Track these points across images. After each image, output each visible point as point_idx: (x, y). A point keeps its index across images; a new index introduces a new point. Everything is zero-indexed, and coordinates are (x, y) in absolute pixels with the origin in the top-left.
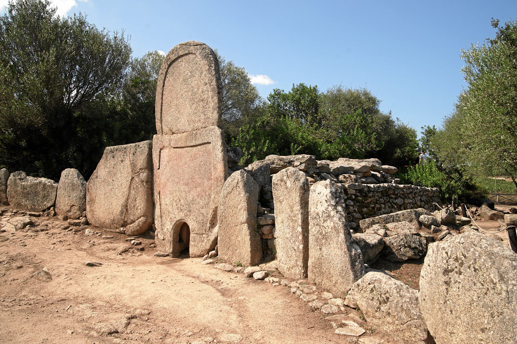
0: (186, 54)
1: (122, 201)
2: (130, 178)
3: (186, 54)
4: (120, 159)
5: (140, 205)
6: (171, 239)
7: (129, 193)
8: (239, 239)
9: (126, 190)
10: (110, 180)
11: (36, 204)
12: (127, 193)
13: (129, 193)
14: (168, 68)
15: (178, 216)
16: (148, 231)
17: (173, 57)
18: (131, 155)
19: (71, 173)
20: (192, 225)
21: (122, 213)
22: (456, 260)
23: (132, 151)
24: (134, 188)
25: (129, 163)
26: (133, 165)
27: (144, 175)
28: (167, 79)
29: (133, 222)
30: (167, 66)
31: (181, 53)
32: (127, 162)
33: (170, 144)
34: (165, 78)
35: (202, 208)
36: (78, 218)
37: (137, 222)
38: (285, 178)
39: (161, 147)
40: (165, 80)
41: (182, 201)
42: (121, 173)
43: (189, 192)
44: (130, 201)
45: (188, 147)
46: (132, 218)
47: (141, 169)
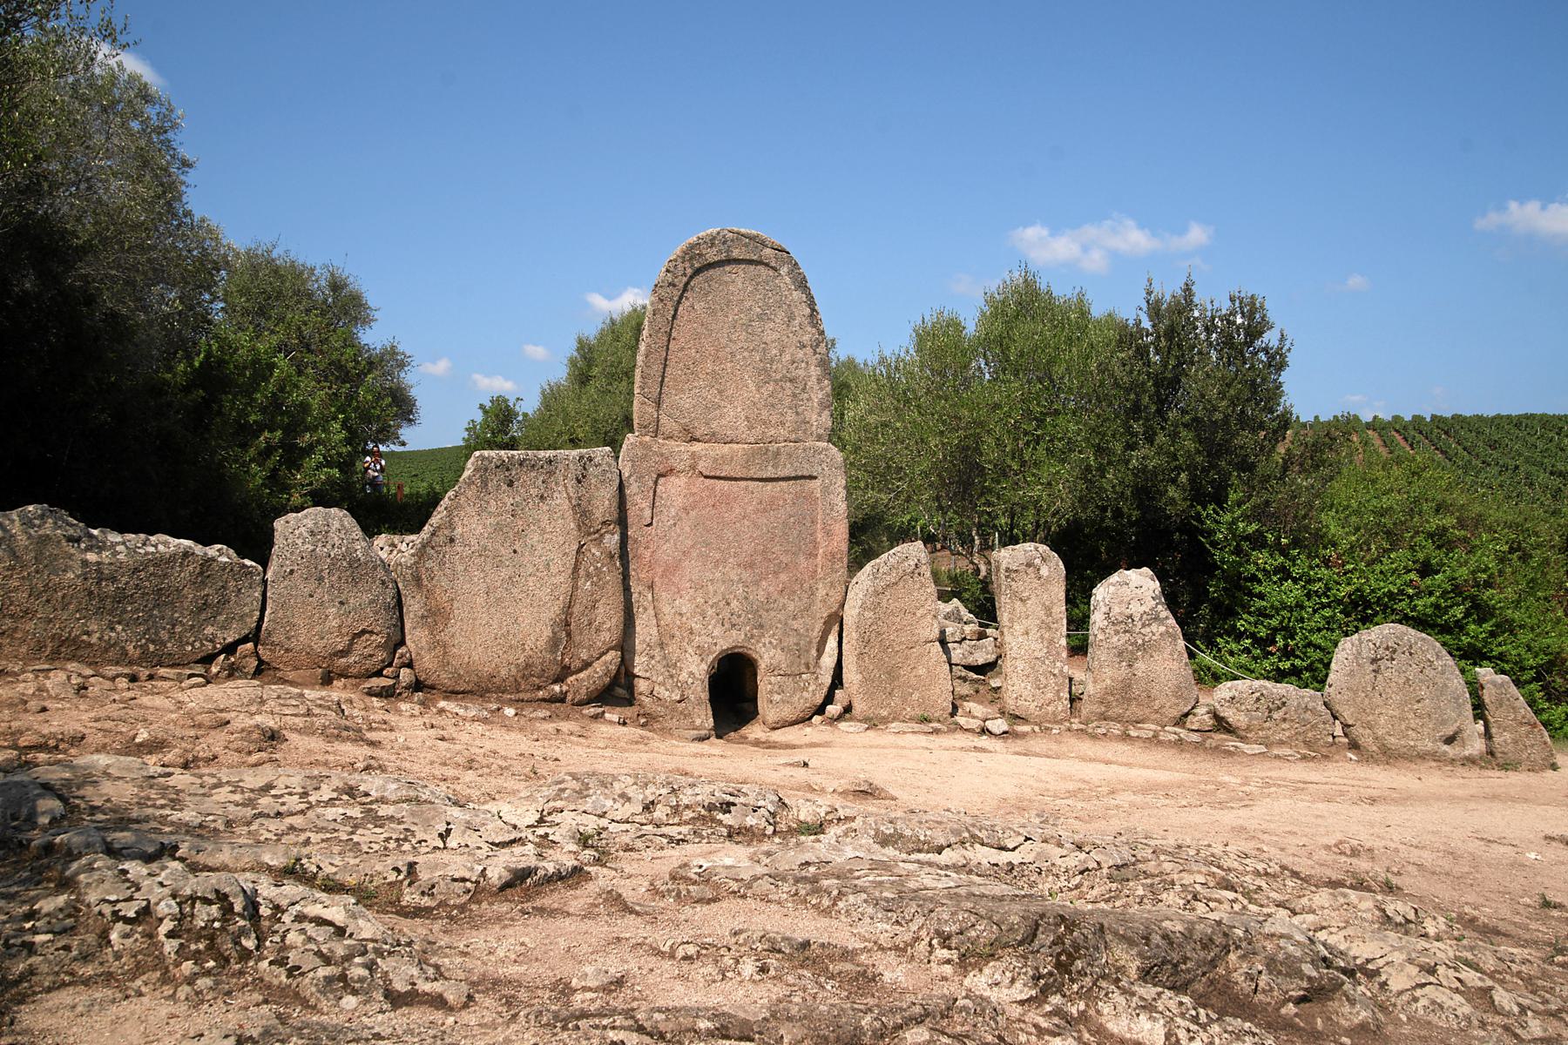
0: (750, 262)
1: (554, 610)
2: (575, 547)
3: (750, 262)
4: (534, 492)
5: (608, 619)
6: (705, 696)
7: (575, 588)
8: (921, 671)
9: (562, 580)
10: (505, 552)
11: (164, 635)
12: (566, 588)
13: (575, 588)
14: (691, 277)
15: (725, 641)
16: (618, 690)
17: (712, 255)
18: (571, 483)
19: (336, 525)
20: (767, 656)
21: (554, 643)
22: (1387, 648)
23: (575, 469)
24: (588, 575)
25: (566, 505)
26: (582, 513)
27: (612, 540)
28: (686, 304)
29: (587, 665)
30: (689, 271)
31: (735, 254)
32: (560, 501)
33: (693, 467)
34: (681, 297)
35: (795, 618)
36: (379, 674)
37: (598, 666)
38: (1038, 561)
39: (662, 469)
40: (679, 302)
41: (734, 604)
42: (543, 532)
43: (757, 583)
44: (576, 609)
45: (752, 479)
46: (584, 656)
47: (604, 523)
